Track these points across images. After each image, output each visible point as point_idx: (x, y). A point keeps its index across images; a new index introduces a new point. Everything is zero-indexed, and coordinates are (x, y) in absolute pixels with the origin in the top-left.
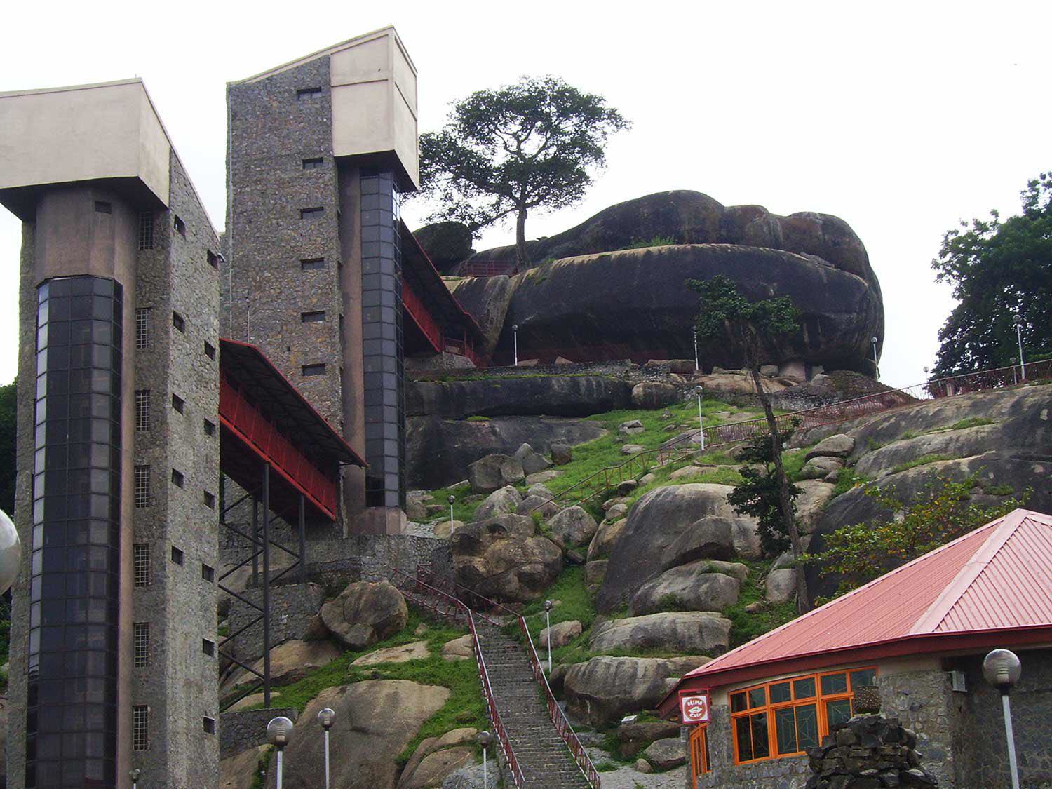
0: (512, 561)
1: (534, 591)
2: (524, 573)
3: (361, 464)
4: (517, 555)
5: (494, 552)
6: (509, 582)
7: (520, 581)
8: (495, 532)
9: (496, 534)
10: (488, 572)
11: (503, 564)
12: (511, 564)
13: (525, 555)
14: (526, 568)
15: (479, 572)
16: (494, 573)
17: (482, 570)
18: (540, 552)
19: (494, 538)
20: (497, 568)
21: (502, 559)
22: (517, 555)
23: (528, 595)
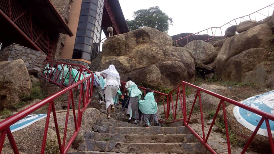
0: (154, 57)
2: (166, 65)
3: (71, 35)
4: (159, 54)
5: (137, 51)
6: (151, 72)
8: (140, 38)
9: (141, 40)
10: (131, 66)
11: (145, 61)
12: (153, 59)
13: (165, 54)
14: (168, 62)
15: (123, 65)
16: (137, 67)
19: (138, 43)
20: (139, 63)
21: (145, 55)
22: (159, 54)
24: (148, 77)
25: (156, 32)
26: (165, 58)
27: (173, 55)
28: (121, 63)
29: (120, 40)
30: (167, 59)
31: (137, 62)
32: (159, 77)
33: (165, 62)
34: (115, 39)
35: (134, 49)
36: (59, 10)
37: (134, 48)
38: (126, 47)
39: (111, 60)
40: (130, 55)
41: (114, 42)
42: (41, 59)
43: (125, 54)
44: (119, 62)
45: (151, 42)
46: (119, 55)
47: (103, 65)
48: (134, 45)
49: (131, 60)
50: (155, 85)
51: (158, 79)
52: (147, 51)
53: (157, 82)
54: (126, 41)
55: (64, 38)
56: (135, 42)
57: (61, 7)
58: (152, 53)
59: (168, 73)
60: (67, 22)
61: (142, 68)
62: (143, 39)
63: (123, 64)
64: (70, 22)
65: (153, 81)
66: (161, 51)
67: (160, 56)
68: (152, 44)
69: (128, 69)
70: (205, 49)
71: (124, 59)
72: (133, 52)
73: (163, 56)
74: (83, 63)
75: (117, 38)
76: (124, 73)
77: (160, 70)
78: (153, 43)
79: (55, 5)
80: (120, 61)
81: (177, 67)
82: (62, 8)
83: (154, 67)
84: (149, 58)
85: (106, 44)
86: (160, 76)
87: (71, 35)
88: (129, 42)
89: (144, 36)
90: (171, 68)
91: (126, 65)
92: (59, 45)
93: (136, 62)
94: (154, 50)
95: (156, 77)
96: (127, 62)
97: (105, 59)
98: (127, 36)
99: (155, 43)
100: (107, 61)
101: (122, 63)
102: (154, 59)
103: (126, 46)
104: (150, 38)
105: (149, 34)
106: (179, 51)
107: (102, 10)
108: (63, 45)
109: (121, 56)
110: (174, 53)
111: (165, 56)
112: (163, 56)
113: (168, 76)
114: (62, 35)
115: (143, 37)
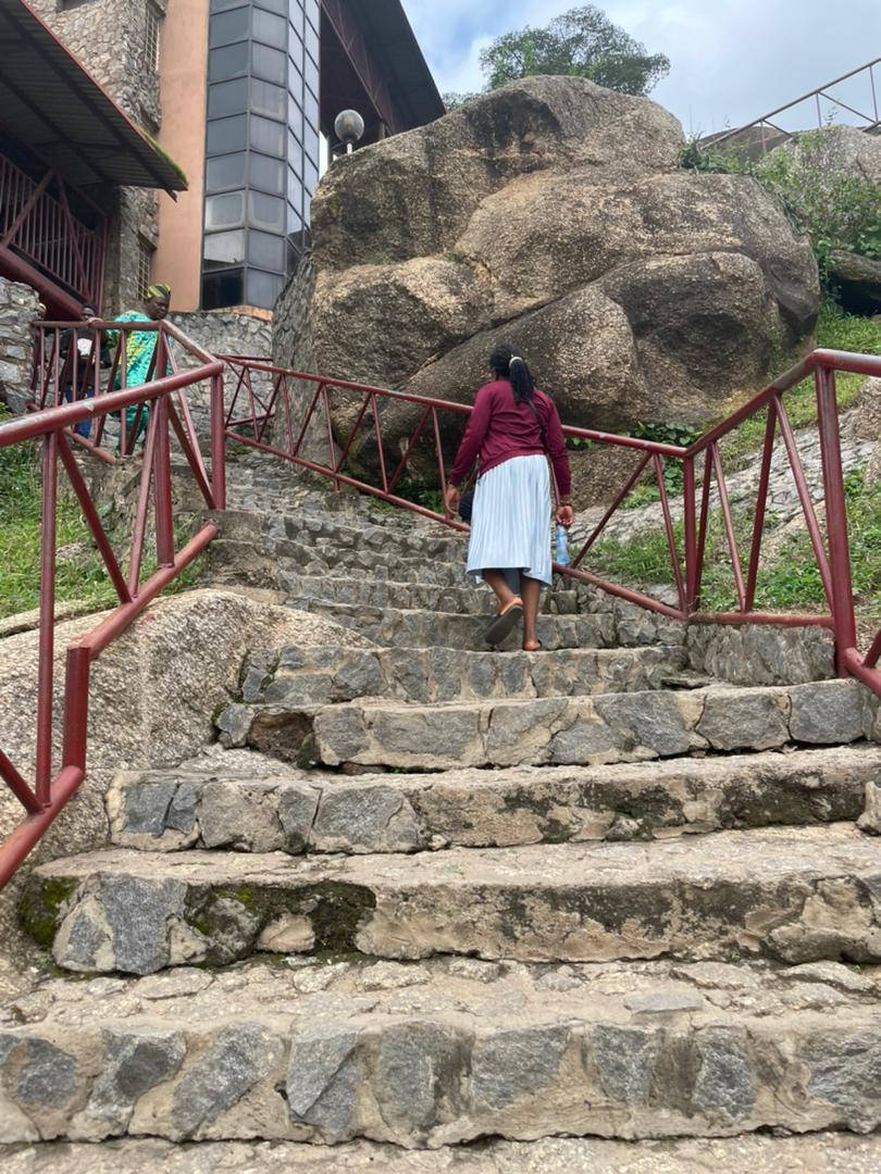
0: (589, 243)
1: (713, 382)
3: (173, 181)
5: (496, 219)
7: (639, 329)
8: (504, 144)
9: (513, 152)
10: (471, 308)
11: (544, 268)
13: (648, 220)
15: (426, 310)
17: (441, 299)
18: (725, 216)
19: (498, 172)
20: (508, 286)
21: (540, 238)
23: (688, 407)
24: (563, 357)
25: (595, 99)
26: (650, 242)
27: (700, 222)
28: (413, 298)
29: (396, 167)
30: (664, 248)
31: (502, 283)
32: (625, 350)
33: (652, 265)
34: (370, 163)
35: (478, 212)
36: (105, 68)
37: (476, 207)
38: (433, 204)
39: (362, 286)
40: (462, 246)
41: (368, 183)
42: (15, 320)
43: (433, 248)
44: (403, 291)
45: (571, 159)
46: (403, 255)
47: (325, 317)
48: (476, 186)
49: (469, 276)
50: (603, 397)
51: (617, 364)
52: (548, 215)
53: (613, 381)
54: (431, 166)
55: (152, 210)
56: (478, 173)
57: (110, 50)
58: (577, 221)
59: (674, 323)
60: (155, 129)
61: (530, 310)
62: (526, 147)
63: (426, 300)
64: (166, 128)
65: (593, 379)
66: (627, 201)
67: (624, 233)
68: (576, 171)
69: (456, 324)
70: (864, 171)
71: (428, 275)
72: (473, 230)
73: (641, 234)
74: (243, 323)
75: (381, 160)
76: (432, 351)
77: (628, 309)
78: (580, 163)
79: (82, 42)
80: (410, 285)
81: (721, 286)
82: (117, 56)
83: (591, 298)
84: (560, 251)
85: (329, 201)
86: (631, 343)
87: (173, 181)
88: (450, 171)
89: (528, 130)
90: (688, 295)
91: (442, 302)
92: (129, 247)
93: (494, 280)
94: (587, 201)
95: (610, 352)
96: (444, 289)
97: (331, 286)
98: (432, 139)
99: (590, 162)
100: (342, 292)
101: (420, 295)
102: (593, 253)
103: (433, 196)
104: (561, 136)
105: (555, 111)
106: (727, 196)
107: (314, 45)
108: (149, 248)
109: (413, 256)
110: (700, 207)
111: (652, 231)
112: (641, 234)
113: (673, 341)
114: (136, 197)
115: (522, 136)
